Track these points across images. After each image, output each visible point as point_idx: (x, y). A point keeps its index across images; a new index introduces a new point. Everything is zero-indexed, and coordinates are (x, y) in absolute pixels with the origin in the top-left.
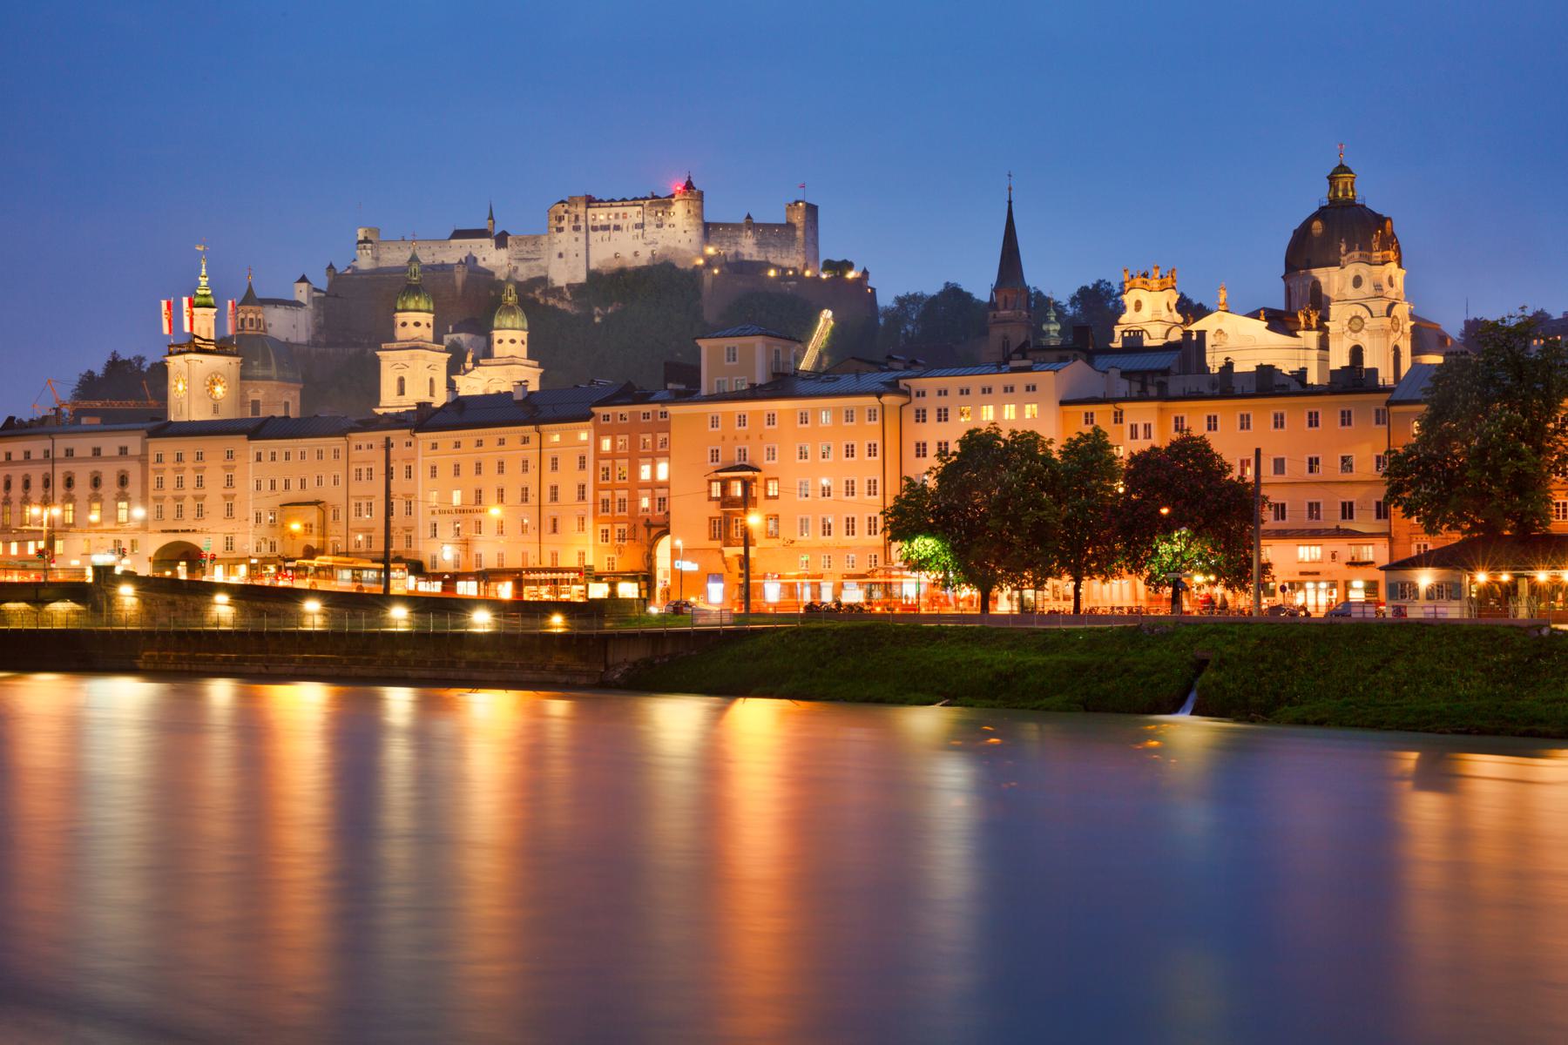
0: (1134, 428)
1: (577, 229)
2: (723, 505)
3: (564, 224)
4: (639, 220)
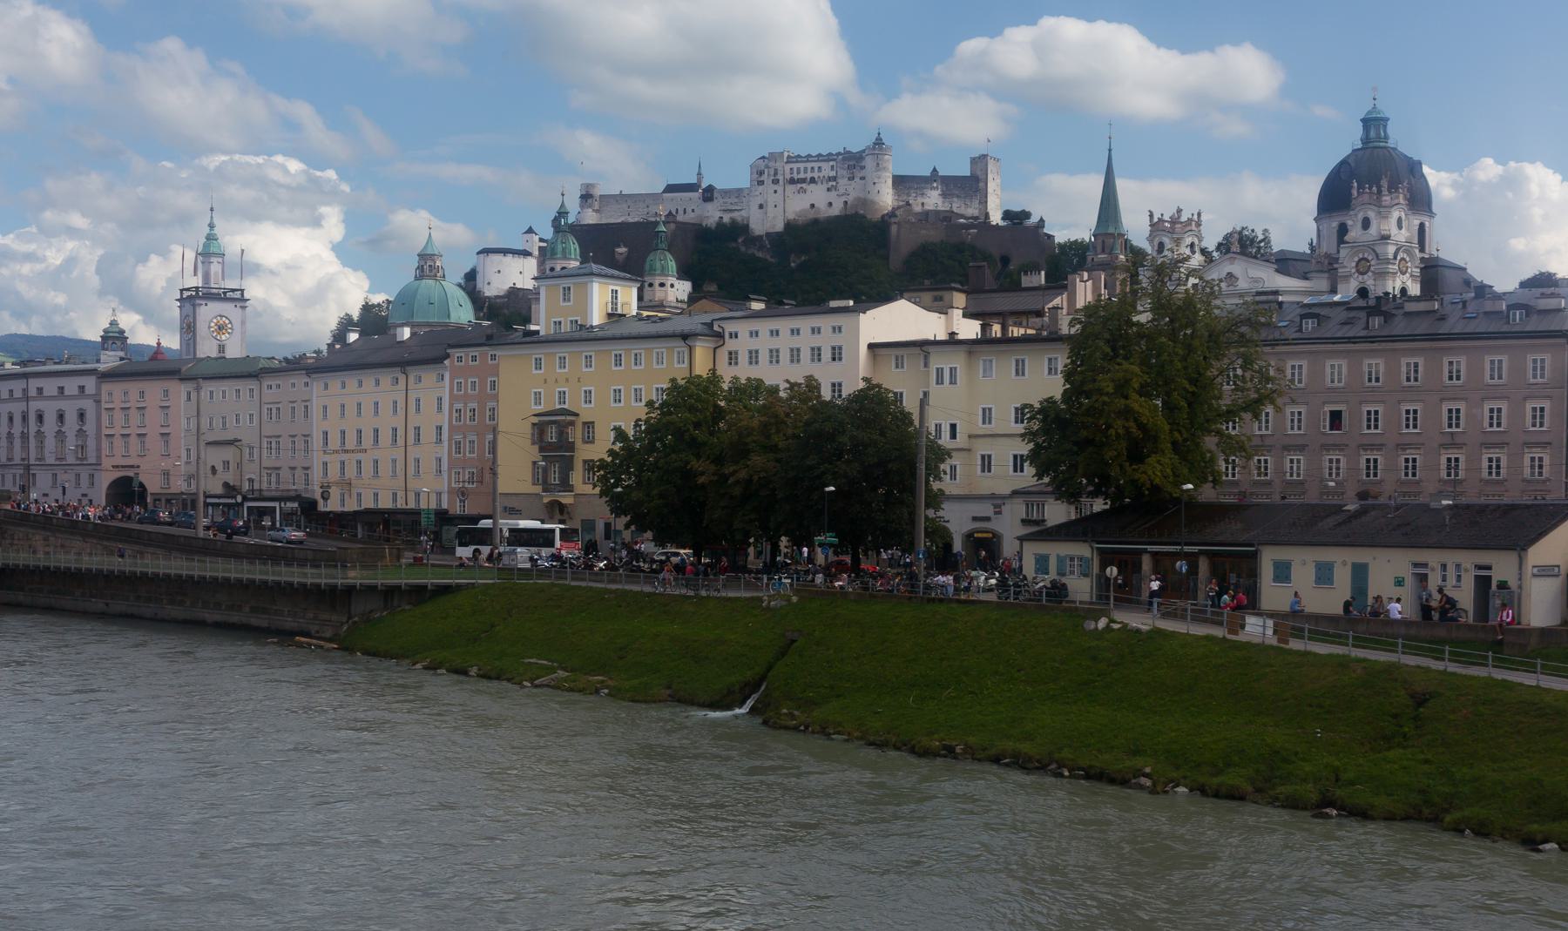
0: (940, 372)
1: (776, 182)
2: (542, 449)
3: (764, 177)
4: (833, 174)
